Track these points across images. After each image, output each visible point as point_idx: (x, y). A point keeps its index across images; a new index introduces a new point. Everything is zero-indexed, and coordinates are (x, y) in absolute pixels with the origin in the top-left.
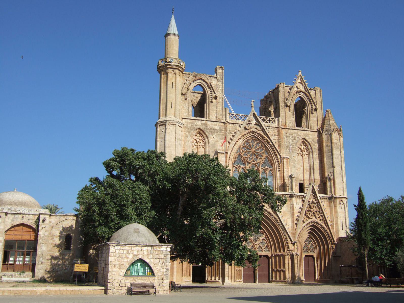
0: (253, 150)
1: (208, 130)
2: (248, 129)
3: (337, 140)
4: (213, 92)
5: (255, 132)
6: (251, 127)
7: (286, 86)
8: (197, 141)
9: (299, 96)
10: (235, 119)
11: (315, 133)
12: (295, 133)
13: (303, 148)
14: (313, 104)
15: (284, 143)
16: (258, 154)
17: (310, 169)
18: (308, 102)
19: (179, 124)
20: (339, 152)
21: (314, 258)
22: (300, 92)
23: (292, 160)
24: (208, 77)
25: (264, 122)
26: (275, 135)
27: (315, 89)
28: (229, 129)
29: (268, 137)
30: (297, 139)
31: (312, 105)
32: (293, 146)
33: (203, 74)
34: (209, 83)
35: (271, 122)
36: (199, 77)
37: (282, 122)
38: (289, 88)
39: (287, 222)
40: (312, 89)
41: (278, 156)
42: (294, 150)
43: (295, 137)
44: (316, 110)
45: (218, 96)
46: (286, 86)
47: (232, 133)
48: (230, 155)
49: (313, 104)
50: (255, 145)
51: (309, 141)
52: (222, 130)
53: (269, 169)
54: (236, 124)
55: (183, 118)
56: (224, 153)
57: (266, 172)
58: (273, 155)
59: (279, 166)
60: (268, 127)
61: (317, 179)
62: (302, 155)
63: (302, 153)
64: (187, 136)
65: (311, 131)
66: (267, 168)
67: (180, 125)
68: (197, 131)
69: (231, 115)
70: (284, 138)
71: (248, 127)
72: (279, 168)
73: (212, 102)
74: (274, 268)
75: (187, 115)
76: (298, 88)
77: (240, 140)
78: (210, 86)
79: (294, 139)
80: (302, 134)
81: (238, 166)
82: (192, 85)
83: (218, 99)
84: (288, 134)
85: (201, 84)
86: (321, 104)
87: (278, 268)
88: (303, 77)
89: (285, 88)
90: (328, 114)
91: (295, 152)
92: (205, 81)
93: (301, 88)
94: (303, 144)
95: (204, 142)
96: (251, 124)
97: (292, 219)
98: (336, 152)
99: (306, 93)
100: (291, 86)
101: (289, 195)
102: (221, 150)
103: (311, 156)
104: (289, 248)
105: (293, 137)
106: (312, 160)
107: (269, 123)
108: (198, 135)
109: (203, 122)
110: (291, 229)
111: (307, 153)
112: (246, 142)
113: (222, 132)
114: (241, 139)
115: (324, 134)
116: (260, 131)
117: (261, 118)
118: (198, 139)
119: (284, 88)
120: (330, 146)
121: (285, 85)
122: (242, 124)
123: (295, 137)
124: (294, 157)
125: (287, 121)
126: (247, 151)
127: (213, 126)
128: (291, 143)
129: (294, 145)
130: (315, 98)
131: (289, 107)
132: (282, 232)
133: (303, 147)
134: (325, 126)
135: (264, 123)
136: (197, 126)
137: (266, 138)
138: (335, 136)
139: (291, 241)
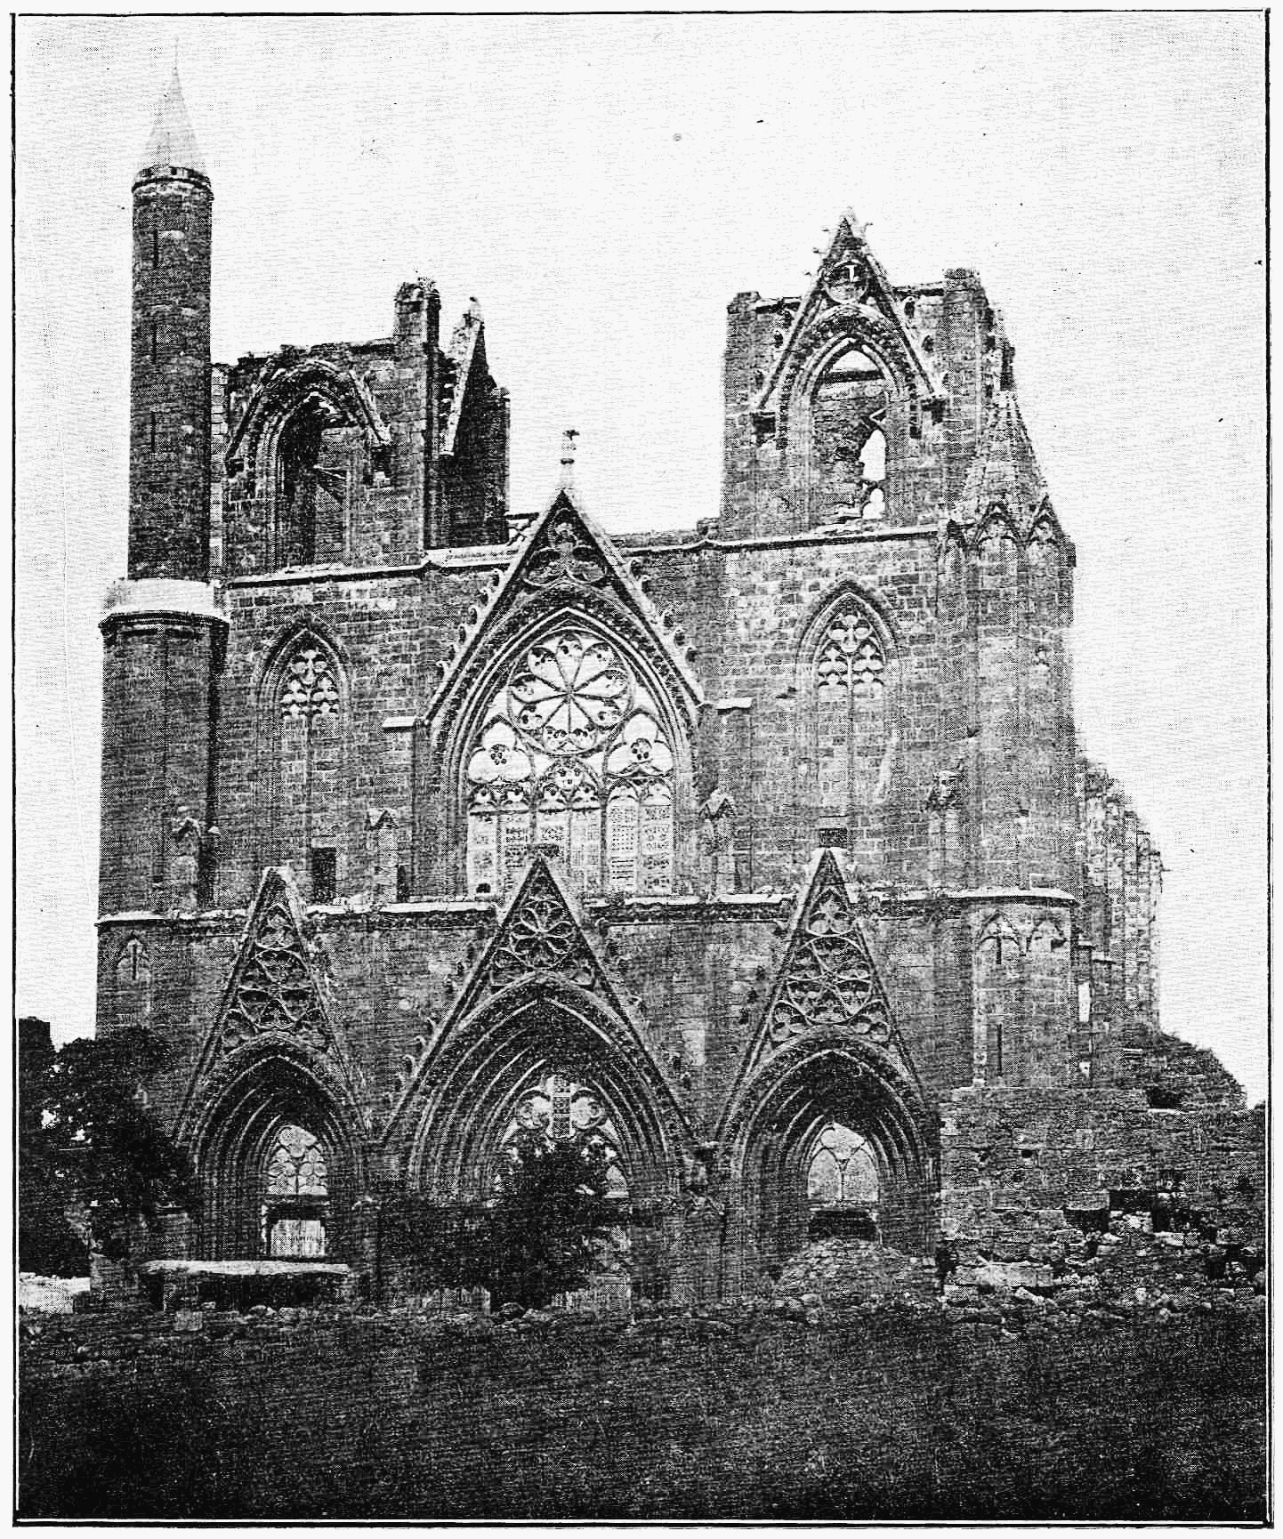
15: (728, 632)
70: (732, 604)
79: (789, 600)
84: (756, 578)
118: (310, 673)
122: (504, 567)
127: (366, 599)
128: (773, 622)
129: (790, 631)
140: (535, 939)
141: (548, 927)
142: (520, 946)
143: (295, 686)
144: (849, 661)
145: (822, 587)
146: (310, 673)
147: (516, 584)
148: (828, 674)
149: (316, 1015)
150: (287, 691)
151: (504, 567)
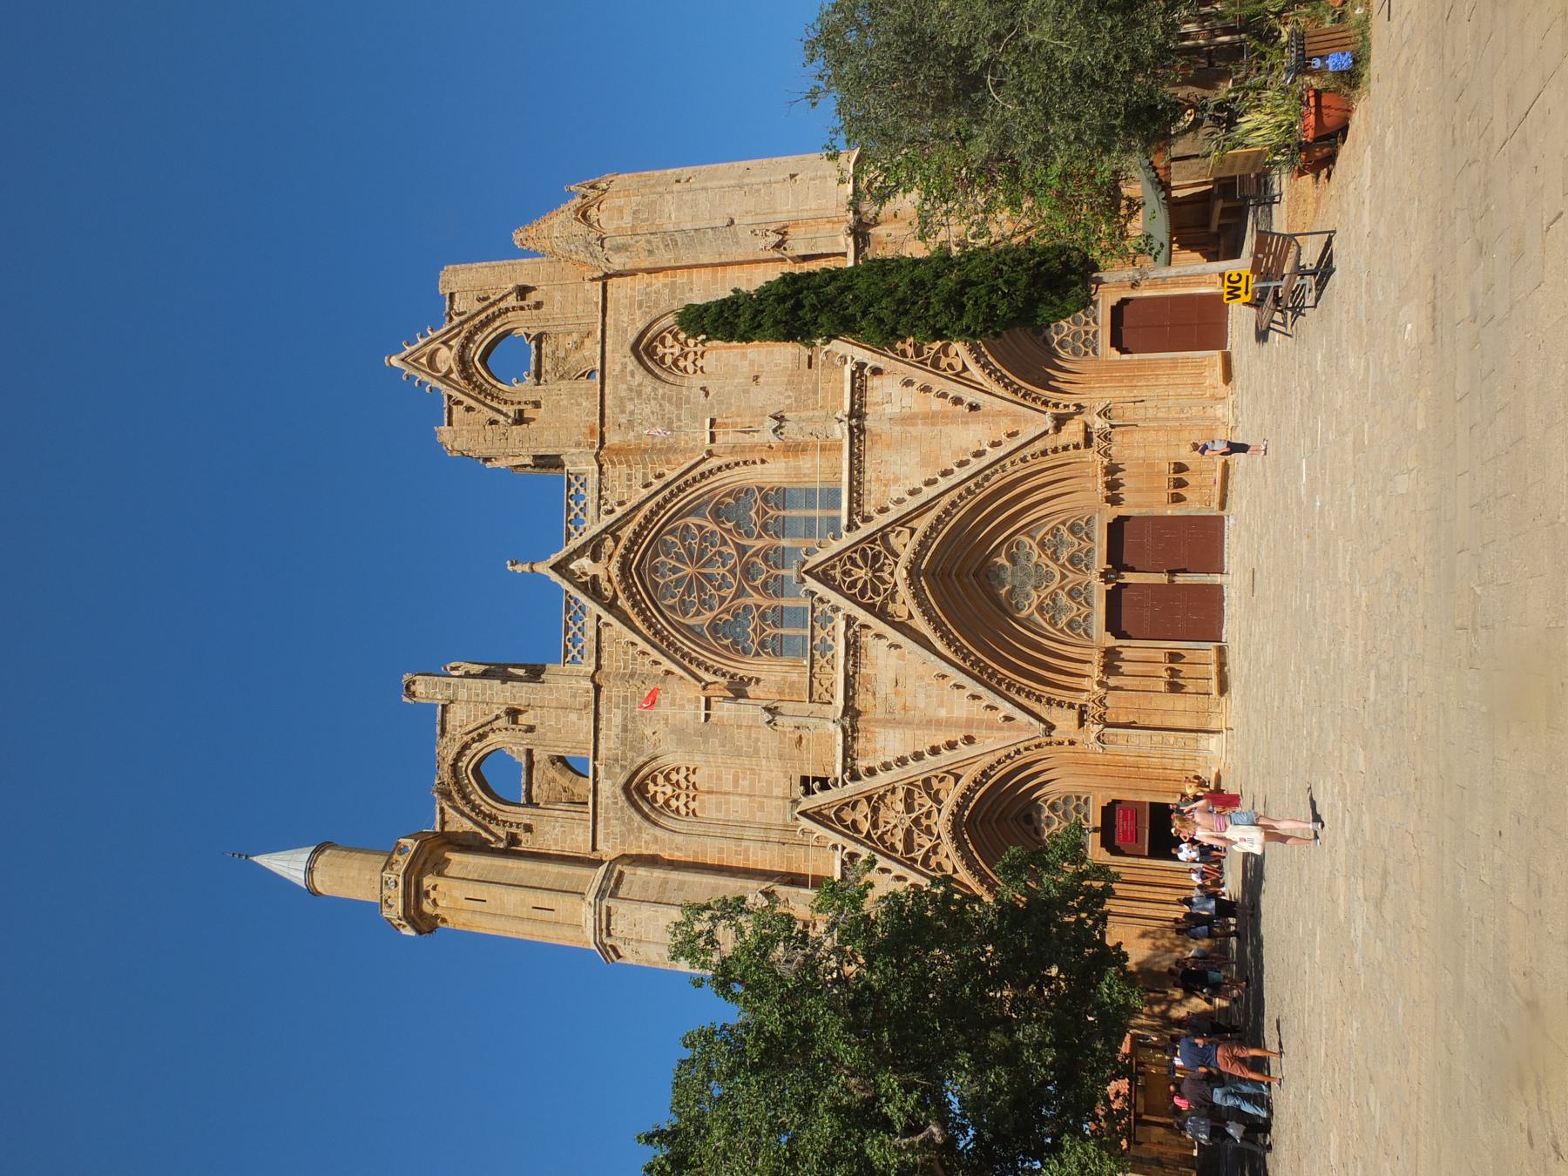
0: (688, 570)
1: (629, 754)
3: (620, 210)
8: (673, 796)
9: (478, 365)
10: (581, 641)
12: (616, 387)
14: (503, 305)
16: (707, 547)
18: (497, 324)
21: (1124, 302)
23: (720, 402)
25: (583, 522)
26: (630, 480)
27: (448, 296)
28: (618, 668)
29: (638, 507)
31: (507, 310)
32: (663, 397)
34: (467, 738)
35: (582, 491)
37: (580, 445)
39: (968, 449)
41: (703, 468)
42: (681, 393)
44: (523, 291)
46: (446, 419)
49: (503, 305)
50: (673, 563)
51: (641, 326)
58: (703, 487)
60: (599, 508)
62: (699, 353)
64: (656, 837)
66: (757, 513)
69: (569, 658)
72: (754, 463)
73: (531, 729)
75: (581, 831)
79: (639, 394)
80: (618, 356)
81: (751, 633)
83: (515, 704)
84: (623, 419)
85: (471, 766)
88: (409, 349)
91: (690, 388)
93: (446, 358)
95: (673, 769)
100: (446, 398)
102: (698, 708)
104: (1078, 444)
105: (632, 399)
113: (633, 699)
117: (569, 535)
118: (663, 789)
120: (649, 242)
122: (599, 618)
123: (631, 390)
124: (707, 394)
127: (612, 733)
129: (660, 391)
134: (574, 257)
136: (616, 798)
137: (639, 517)
139: (1046, 432)
140: (871, 579)
141: (862, 568)
142: (876, 592)
144: (686, 349)
147: (611, 607)
148: (696, 366)
149: (927, 781)
151: (599, 618)
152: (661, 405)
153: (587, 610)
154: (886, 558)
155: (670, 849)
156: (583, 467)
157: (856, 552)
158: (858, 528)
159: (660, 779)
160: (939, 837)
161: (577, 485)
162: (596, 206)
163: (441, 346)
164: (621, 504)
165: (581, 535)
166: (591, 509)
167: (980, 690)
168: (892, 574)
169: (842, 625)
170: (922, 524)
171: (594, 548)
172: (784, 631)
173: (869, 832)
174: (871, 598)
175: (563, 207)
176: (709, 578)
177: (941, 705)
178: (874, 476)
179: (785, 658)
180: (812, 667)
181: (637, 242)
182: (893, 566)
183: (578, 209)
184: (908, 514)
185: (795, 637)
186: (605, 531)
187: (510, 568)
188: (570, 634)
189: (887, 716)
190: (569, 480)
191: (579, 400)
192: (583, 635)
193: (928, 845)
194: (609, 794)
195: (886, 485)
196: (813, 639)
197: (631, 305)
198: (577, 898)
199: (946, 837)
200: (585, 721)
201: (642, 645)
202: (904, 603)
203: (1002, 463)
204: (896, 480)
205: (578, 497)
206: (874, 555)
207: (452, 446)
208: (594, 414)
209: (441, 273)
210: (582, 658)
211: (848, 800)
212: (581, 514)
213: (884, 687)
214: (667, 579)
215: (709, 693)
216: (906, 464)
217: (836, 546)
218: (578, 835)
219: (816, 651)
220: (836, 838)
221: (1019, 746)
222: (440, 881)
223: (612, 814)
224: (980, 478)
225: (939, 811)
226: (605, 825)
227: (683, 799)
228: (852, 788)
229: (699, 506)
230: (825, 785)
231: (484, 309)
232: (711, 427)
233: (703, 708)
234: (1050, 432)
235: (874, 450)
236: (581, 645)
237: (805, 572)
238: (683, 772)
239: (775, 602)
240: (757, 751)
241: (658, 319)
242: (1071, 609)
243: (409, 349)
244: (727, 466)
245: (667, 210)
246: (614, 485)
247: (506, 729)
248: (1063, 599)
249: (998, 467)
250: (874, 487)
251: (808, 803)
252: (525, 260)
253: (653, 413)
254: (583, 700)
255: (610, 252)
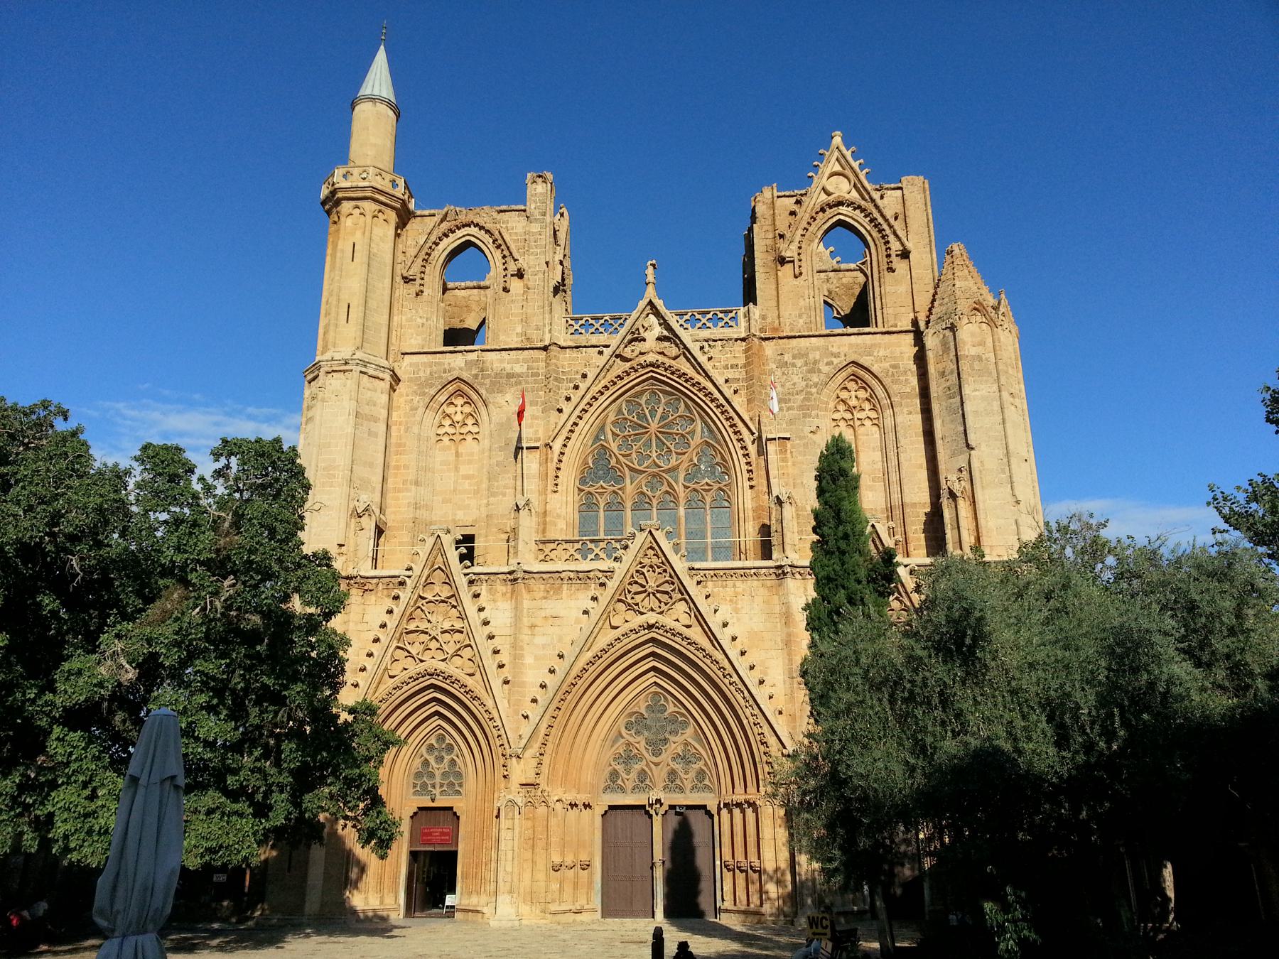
0: (654, 425)
1: (488, 381)
2: (630, 360)
3: (982, 343)
4: (509, 259)
5: (658, 367)
6: (642, 351)
7: (778, 197)
11: (902, 336)
12: (818, 348)
13: (856, 397)
14: (892, 238)
17: (887, 472)
19: (364, 369)
20: (995, 387)
22: (840, 203)
23: (806, 445)
24: (495, 214)
25: (693, 327)
26: (732, 367)
27: (900, 185)
29: (708, 376)
30: (825, 369)
33: (478, 210)
35: (721, 324)
36: (463, 218)
37: (763, 319)
38: (794, 199)
39: (766, 674)
40: (886, 186)
43: (815, 362)
44: (905, 255)
45: (525, 266)
46: (783, 193)
47: (571, 381)
48: (562, 453)
49: (892, 238)
50: (660, 411)
51: (874, 369)
52: (537, 375)
53: (716, 486)
54: (585, 347)
55: (402, 354)
56: (538, 448)
57: (703, 497)
58: (728, 434)
59: (751, 471)
60: (706, 341)
61: (914, 505)
62: (851, 423)
63: (853, 414)
64: (416, 409)
65: (883, 333)
67: (371, 372)
68: (451, 388)
69: (571, 322)
71: (633, 351)
72: (750, 479)
73: (506, 290)
74: (727, 856)
75: (420, 342)
76: (829, 194)
77: (602, 398)
78: (500, 242)
79: (811, 371)
80: (844, 349)
81: (599, 485)
82: (441, 247)
84: (787, 357)
86: (929, 231)
87: (740, 856)
88: (848, 154)
89: (779, 202)
90: (951, 260)
92: (482, 228)
93: (842, 188)
94: (857, 383)
96: (644, 340)
97: (787, 661)
98: (977, 393)
99: (863, 203)
101: (772, 570)
103: (889, 422)
105: (806, 364)
106: (891, 436)
107: (714, 330)
108: (459, 401)
109: (473, 356)
110: (782, 698)
111: (873, 415)
112: (627, 401)
113: (536, 382)
114: (607, 393)
115: (930, 332)
116: (675, 358)
117: (681, 315)
118: (459, 413)
119: (773, 202)
121: (776, 194)
125: (785, 314)
126: (632, 432)
127: (506, 365)
129: (814, 390)
130: (901, 217)
131: (793, 261)
132: (747, 713)
133: (855, 395)
135: (695, 331)
136: (449, 371)
137: (701, 379)
138: (970, 331)
143: (447, 422)
145: (835, 363)
146: (459, 413)
150: (441, 426)
152: (802, 391)
153: (614, 335)
154: (666, 604)
155: (407, 423)
156: (743, 322)
157: (671, 576)
158: (691, 577)
159: (467, 409)
160: (422, 661)
161: (727, 319)
162: (984, 320)
163: (852, 184)
164: (710, 359)
165: (681, 325)
166: (705, 334)
167: (551, 691)
168: (652, 610)
169: (606, 564)
170: (696, 634)
171: (671, 337)
172: (602, 513)
173: (425, 599)
174: (629, 592)
175: (985, 290)
176: (648, 445)
177: (536, 658)
178: (739, 590)
179: (577, 516)
180: (567, 541)
181: (951, 361)
182: (659, 610)
183: (981, 304)
184: (705, 622)
185: (597, 524)
186: (685, 347)
187: (650, 262)
188: (593, 322)
189: (525, 610)
190: (731, 311)
191: (805, 316)
192: (592, 333)
193: (414, 652)
194: (452, 365)
195: (731, 601)
196: (592, 541)
197: (894, 358)
198: (358, 343)
199: (421, 668)
200: (515, 339)
201: (583, 386)
202: (627, 621)
203: (755, 707)
204: (736, 610)
205: (715, 320)
206: (667, 593)
207: (759, 201)
208: (792, 330)
209: (921, 178)
210: (572, 334)
211: (451, 579)
212: (699, 325)
213: (552, 606)
214: (644, 406)
215: (543, 449)
216: (751, 619)
217: (674, 559)
218: (416, 339)
219: (585, 544)
220: (417, 570)
221: (502, 730)
222: (369, 217)
223: (435, 368)
224: (741, 686)
225: (443, 660)
226: (425, 363)
227: (451, 431)
228: (461, 581)
229: (711, 431)
230: (462, 558)
231: (887, 220)
232: (779, 438)
233: (529, 445)
234: (784, 751)
235: (762, 589)
236: (583, 331)
237: (650, 532)
238: (475, 429)
239: (628, 504)
240: (494, 494)
241: (882, 384)
242: (628, 773)
243: (848, 154)
244: (746, 455)
245: (983, 387)
246: (727, 353)
247: (506, 269)
248: (637, 767)
249: (751, 702)
250: (730, 591)
251: (448, 541)
252: (934, 255)
253: (794, 384)
254: (534, 337)
255: (941, 336)
